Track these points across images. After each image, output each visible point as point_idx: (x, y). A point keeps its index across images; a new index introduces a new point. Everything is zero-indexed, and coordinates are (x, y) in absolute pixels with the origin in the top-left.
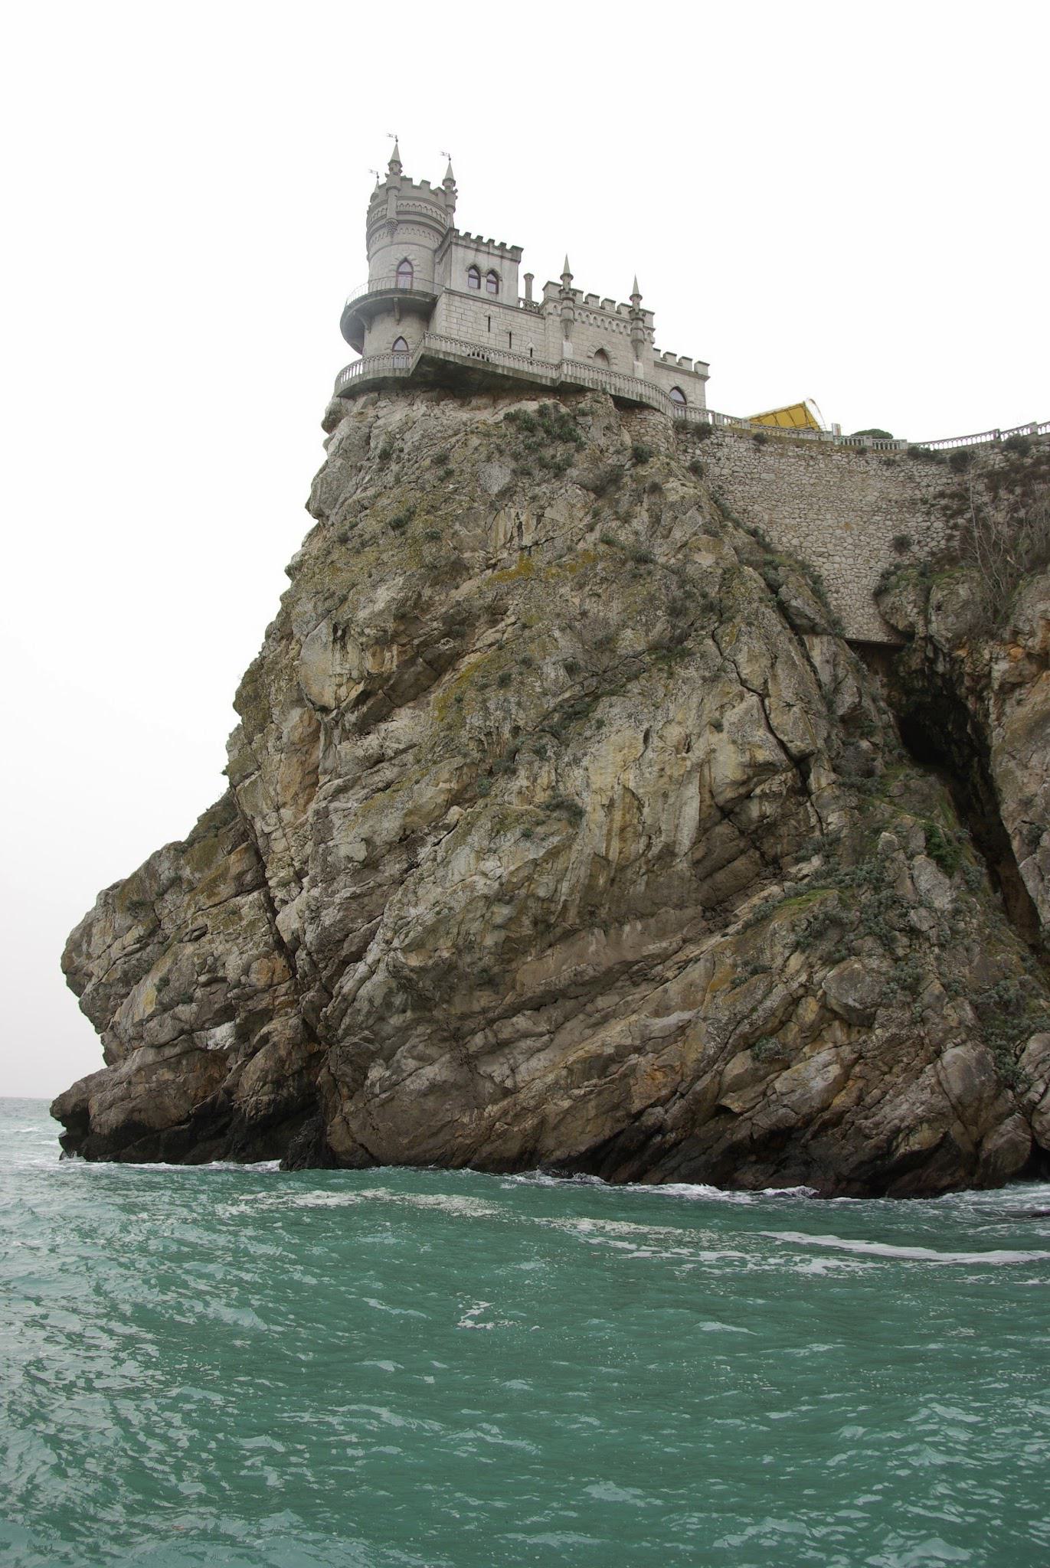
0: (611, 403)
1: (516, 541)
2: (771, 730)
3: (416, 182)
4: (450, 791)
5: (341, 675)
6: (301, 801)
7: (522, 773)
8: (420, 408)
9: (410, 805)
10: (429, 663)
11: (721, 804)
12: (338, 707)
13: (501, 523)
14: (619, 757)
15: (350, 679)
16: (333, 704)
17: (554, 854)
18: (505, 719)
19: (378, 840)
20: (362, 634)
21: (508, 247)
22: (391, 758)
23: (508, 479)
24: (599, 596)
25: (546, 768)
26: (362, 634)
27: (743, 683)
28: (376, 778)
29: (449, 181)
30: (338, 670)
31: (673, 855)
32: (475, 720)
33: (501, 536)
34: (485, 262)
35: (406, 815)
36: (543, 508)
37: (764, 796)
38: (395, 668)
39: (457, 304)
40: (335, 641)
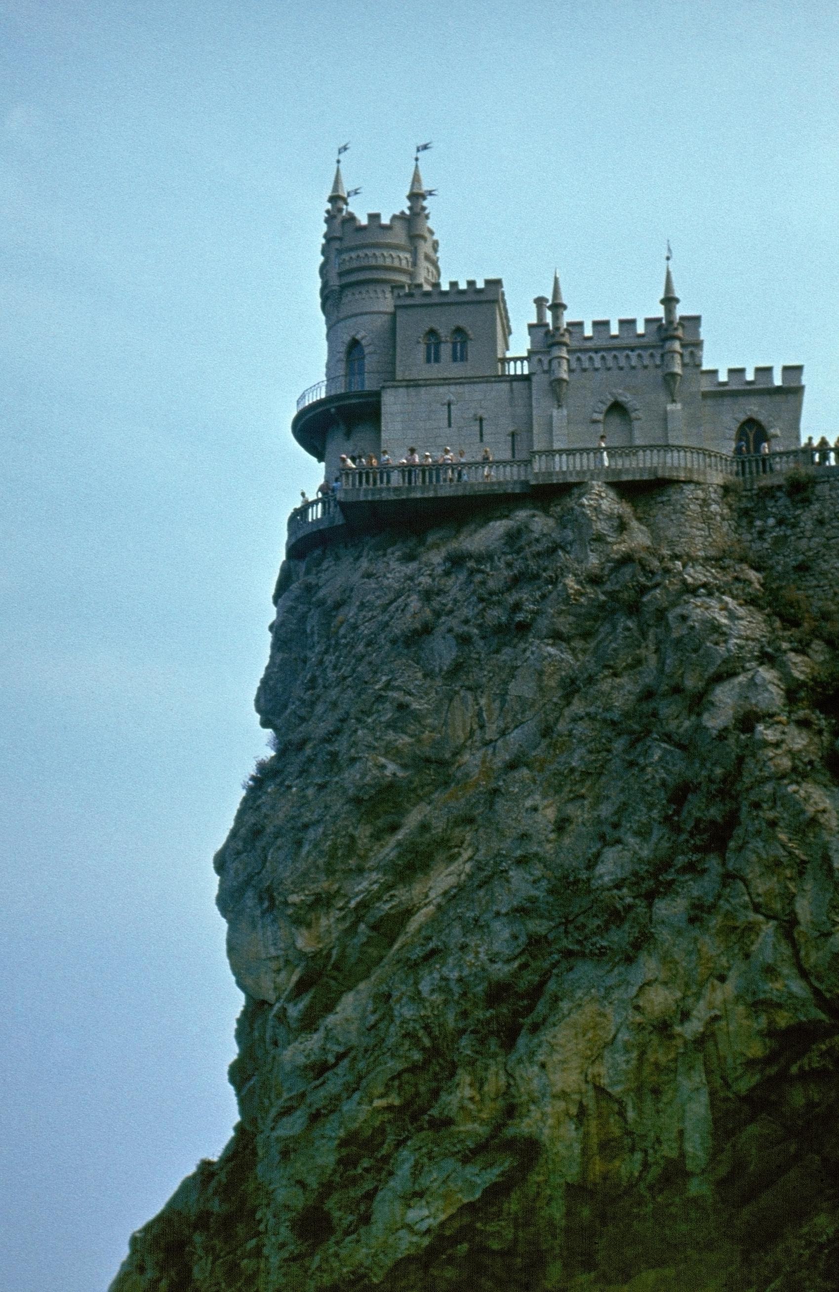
0: (612, 494)
2: (804, 974)
3: (364, 221)
4: (390, 1108)
7: (464, 1077)
9: (342, 1133)
10: (374, 928)
11: (744, 1093)
12: (278, 999)
15: (287, 962)
16: (271, 996)
17: (496, 1192)
18: (446, 1002)
19: (313, 1182)
20: (286, 903)
21: (480, 285)
22: (335, 1065)
23: (454, 653)
24: (583, 797)
25: (493, 1069)
27: (757, 908)
28: (322, 1093)
29: (416, 196)
30: (273, 952)
31: (688, 1175)
35: (340, 1146)
36: (506, 683)
37: (804, 1076)
40: (263, 913)
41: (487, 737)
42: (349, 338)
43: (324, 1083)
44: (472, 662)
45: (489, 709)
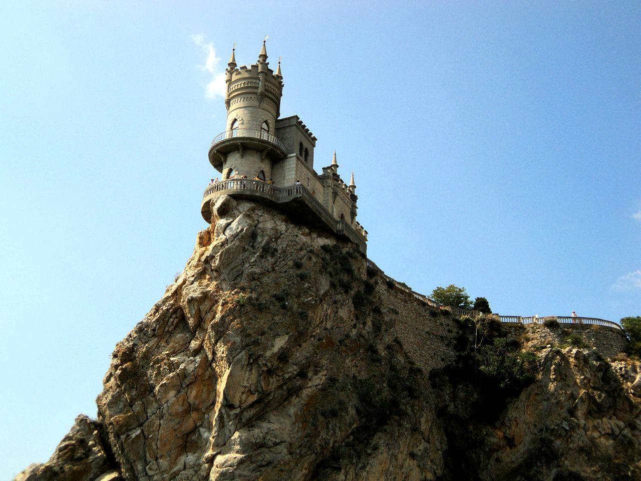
1: (324, 323)
5: (246, 387)
6: (173, 456)
8: (282, 227)
12: (240, 407)
13: (319, 312)
14: (380, 469)
16: (237, 403)
20: (266, 365)
21: (312, 136)
24: (357, 366)
26: (266, 365)
28: (260, 458)
30: (245, 384)
32: (323, 434)
33: (318, 319)
34: (306, 145)
36: (337, 308)
38: (273, 390)
39: (299, 166)
40: (248, 364)
41: (327, 326)
42: (265, 120)
43: (261, 453)
44: (329, 294)
45: (330, 316)
